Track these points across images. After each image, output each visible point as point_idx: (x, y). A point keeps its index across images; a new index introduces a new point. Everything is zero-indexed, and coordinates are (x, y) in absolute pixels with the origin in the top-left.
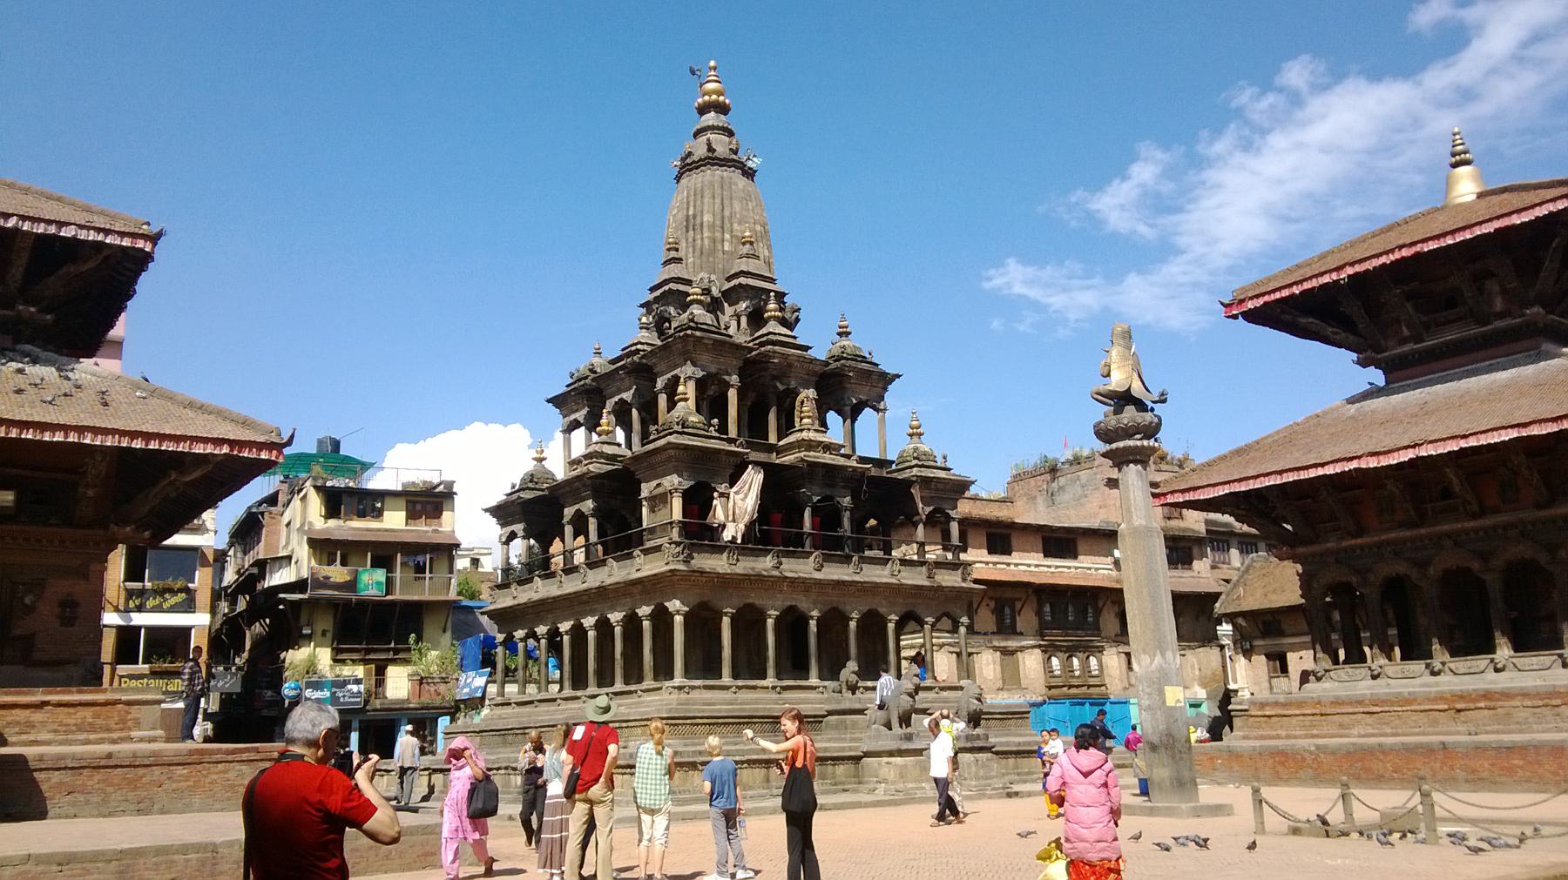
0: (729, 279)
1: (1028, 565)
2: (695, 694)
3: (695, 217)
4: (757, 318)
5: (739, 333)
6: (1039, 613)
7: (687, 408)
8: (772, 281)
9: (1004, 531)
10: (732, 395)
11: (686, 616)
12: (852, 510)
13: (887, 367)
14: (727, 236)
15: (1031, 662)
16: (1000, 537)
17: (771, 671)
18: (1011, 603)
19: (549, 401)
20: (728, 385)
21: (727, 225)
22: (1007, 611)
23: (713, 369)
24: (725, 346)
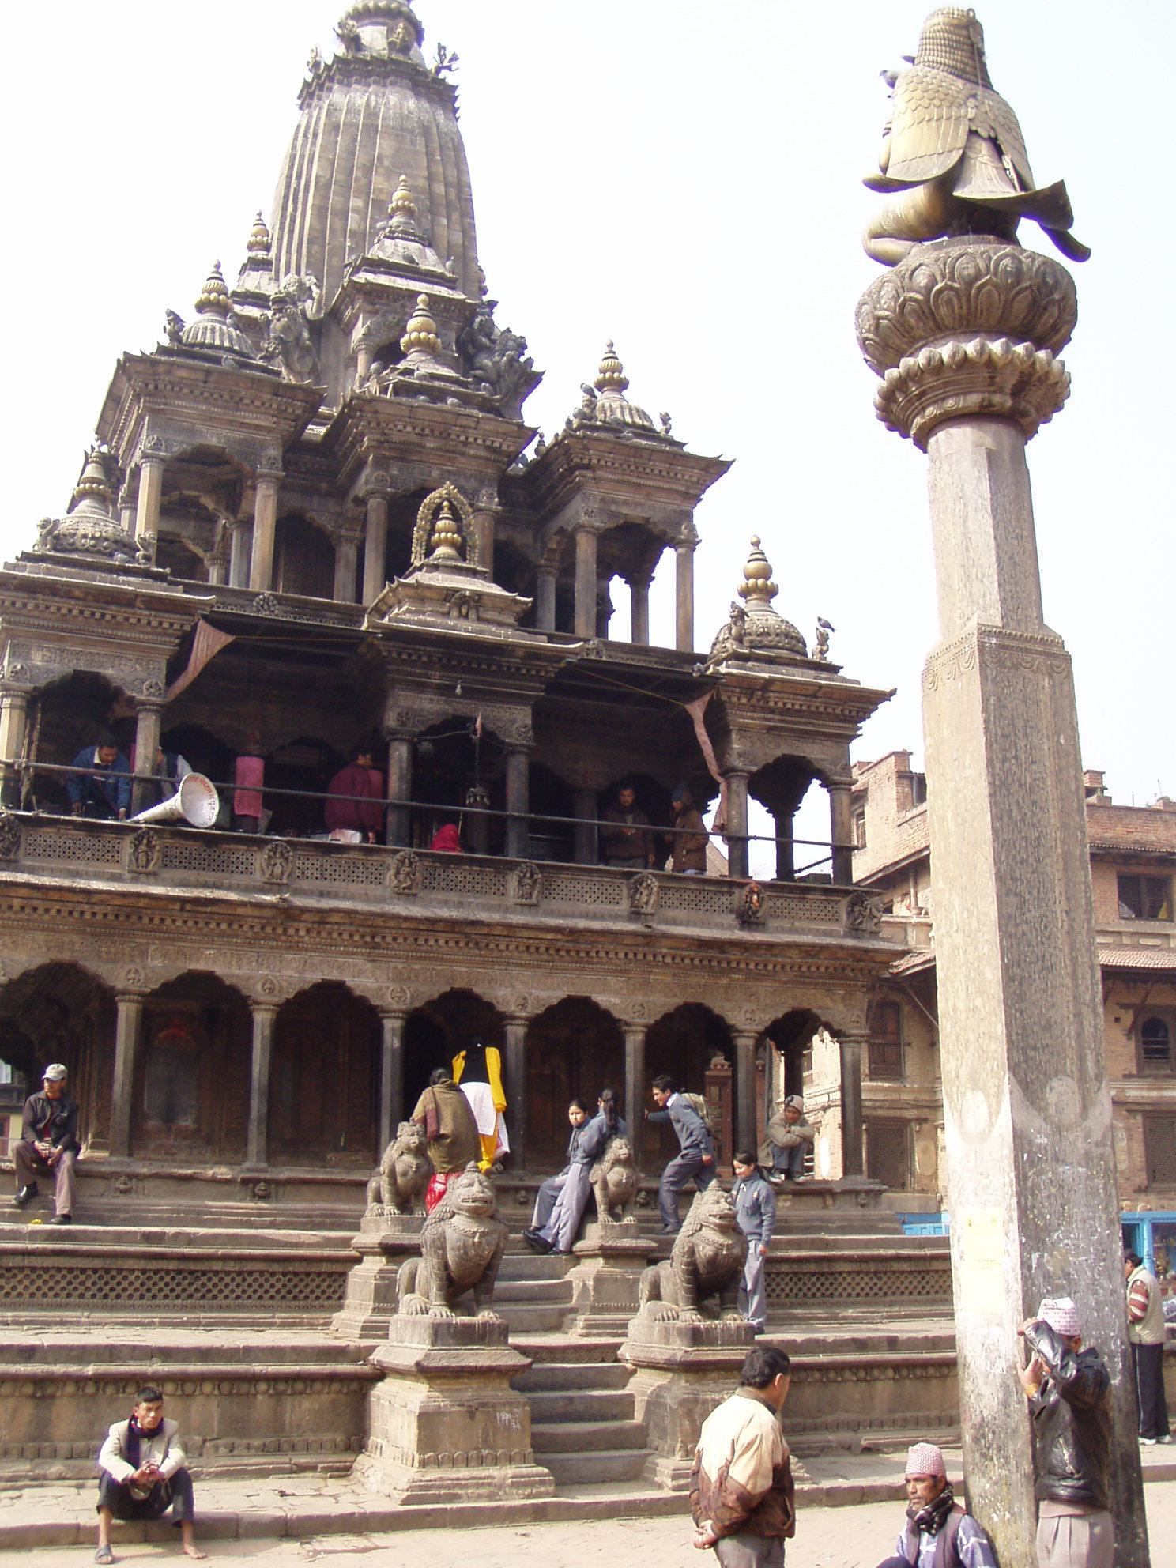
9: (1154, 871)
13: (698, 446)
14: (356, 202)
17: (256, 1140)
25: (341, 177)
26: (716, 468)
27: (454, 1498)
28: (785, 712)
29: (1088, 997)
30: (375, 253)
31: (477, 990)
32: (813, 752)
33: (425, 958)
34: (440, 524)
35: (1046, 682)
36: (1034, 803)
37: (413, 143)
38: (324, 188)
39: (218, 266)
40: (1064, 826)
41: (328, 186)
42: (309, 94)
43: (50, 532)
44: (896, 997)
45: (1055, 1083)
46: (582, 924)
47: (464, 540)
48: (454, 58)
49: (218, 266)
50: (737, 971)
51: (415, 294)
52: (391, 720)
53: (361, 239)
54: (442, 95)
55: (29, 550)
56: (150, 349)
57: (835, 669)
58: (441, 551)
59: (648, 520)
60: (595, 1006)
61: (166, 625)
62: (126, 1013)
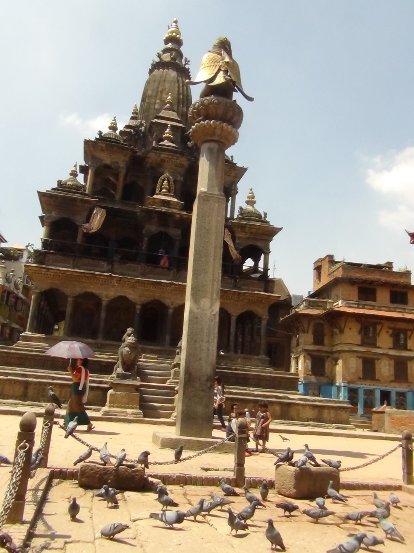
14: (158, 101)
18: (405, 331)
22: (402, 336)
23: (107, 161)
26: (244, 170)
27: (116, 415)
28: (251, 233)
29: (216, 280)
30: (161, 114)
32: (260, 244)
35: (217, 205)
36: (208, 233)
37: (174, 85)
39: (115, 118)
40: (216, 239)
42: (151, 71)
43: (59, 182)
44: (322, 322)
45: (204, 300)
47: (170, 188)
48: (189, 61)
49: (115, 118)
51: (166, 125)
52: (144, 231)
53: (159, 111)
55: (54, 187)
56: (93, 139)
57: (268, 222)
58: (164, 190)
62: (70, 300)
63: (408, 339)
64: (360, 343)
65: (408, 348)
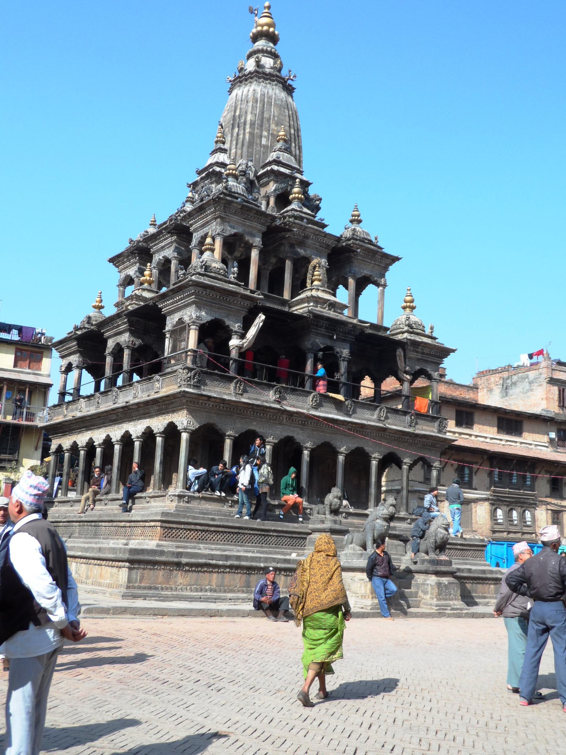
0: (263, 167)
1: (484, 436)
2: (194, 504)
3: (240, 116)
4: (283, 199)
5: (268, 206)
6: (490, 474)
7: (213, 257)
8: (301, 172)
10: (254, 254)
11: (193, 435)
12: (349, 362)
14: (265, 133)
15: (481, 513)
16: (467, 413)
19: (111, 260)
20: (249, 247)
21: (266, 125)
22: (467, 471)
24: (249, 210)
25: (259, 122)
28: (423, 353)
31: (332, 443)
33: (318, 430)
34: (316, 273)
37: (284, 111)
38: (252, 124)
41: (254, 124)
46: (365, 422)
50: (405, 442)
54: (289, 90)
57: (435, 338)
59: (371, 276)
60: (365, 450)
61: (246, 305)
63: (474, 474)
64: (422, 480)
65: (474, 487)
